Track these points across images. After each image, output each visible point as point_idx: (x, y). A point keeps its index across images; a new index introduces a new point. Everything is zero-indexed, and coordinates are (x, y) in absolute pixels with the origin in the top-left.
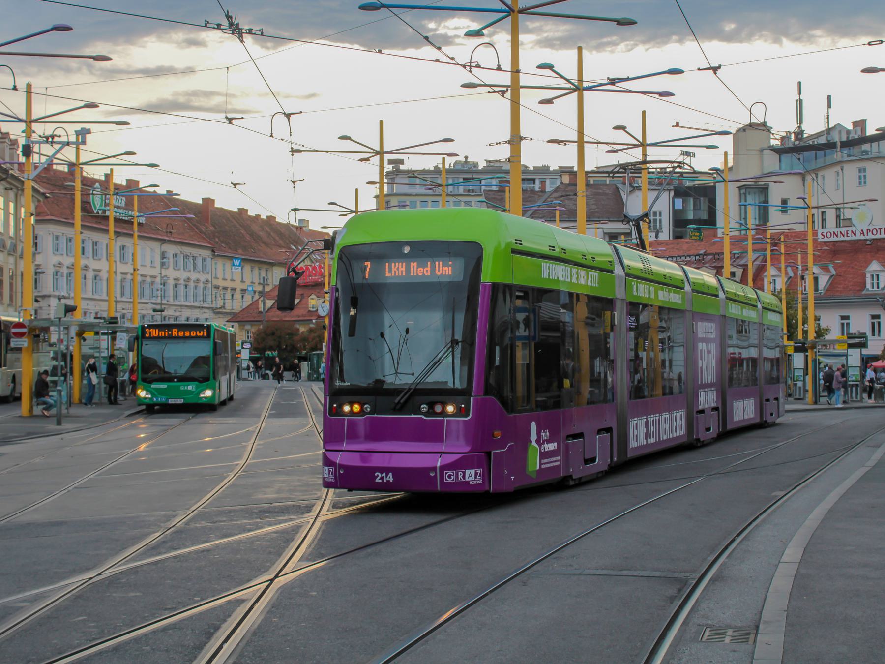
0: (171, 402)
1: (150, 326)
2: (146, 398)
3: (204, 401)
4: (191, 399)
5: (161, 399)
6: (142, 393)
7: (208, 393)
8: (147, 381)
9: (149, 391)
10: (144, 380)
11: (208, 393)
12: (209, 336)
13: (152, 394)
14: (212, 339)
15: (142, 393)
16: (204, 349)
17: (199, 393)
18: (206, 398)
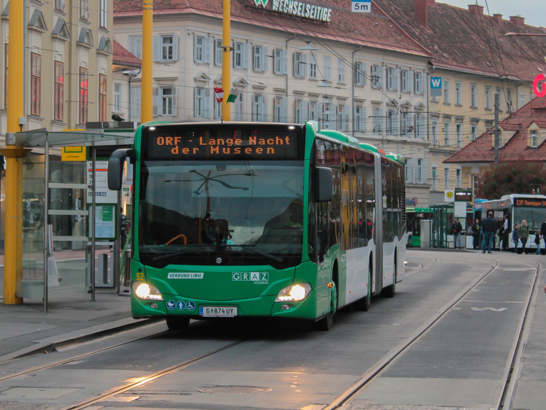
0: (207, 312)
1: (163, 130)
2: (150, 302)
3: (288, 311)
4: (255, 307)
5: (182, 306)
6: (143, 290)
7: (297, 293)
8: (154, 261)
9: (157, 286)
10: (146, 259)
11: (297, 293)
12: (300, 157)
13: (165, 293)
14: (307, 163)
15: (143, 290)
16: (284, 183)
17: (276, 295)
18: (291, 304)
